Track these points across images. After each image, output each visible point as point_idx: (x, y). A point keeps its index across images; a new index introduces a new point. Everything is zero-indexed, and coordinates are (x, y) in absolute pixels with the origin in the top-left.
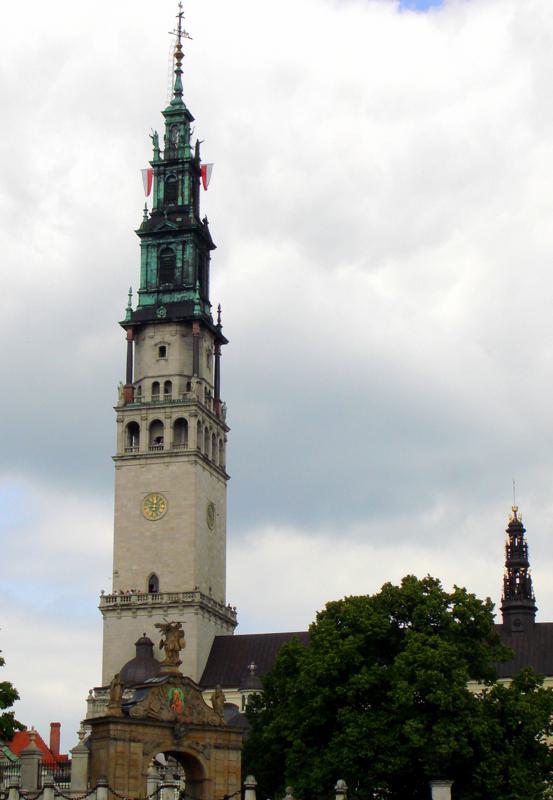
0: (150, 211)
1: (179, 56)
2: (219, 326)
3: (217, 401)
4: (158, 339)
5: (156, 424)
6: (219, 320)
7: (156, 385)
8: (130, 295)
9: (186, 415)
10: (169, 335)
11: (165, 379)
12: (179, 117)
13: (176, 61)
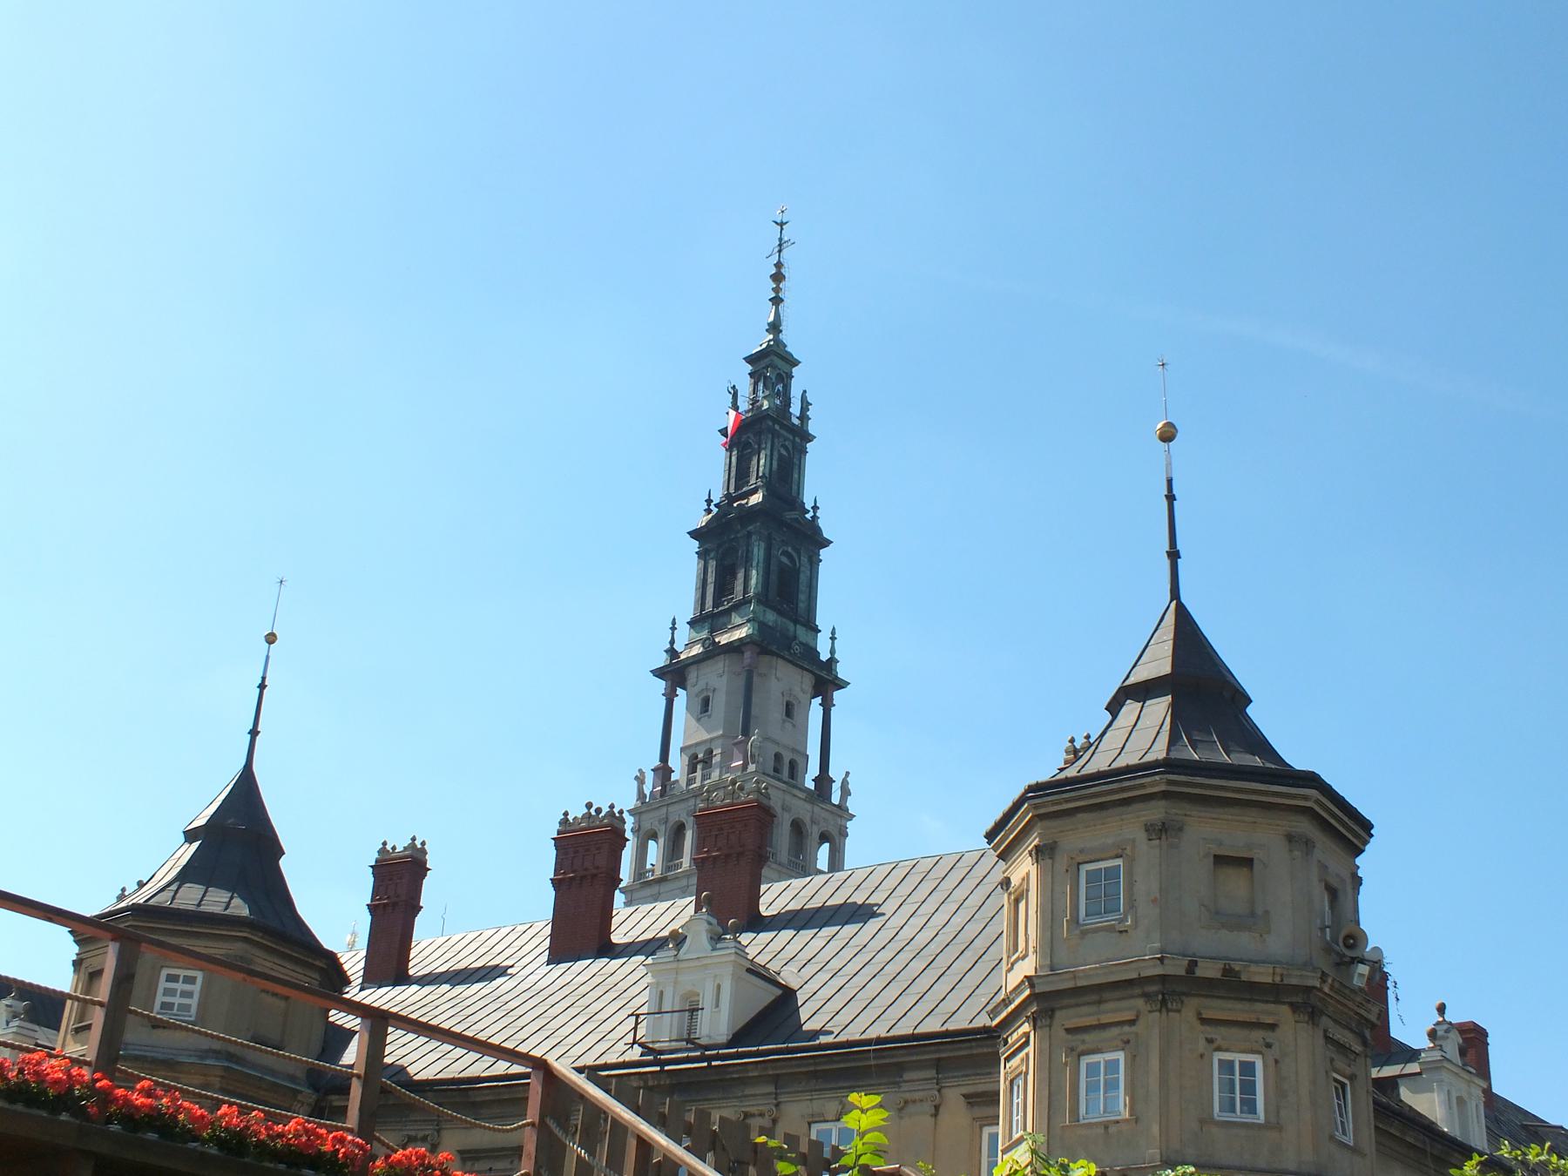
1: (778, 277)
2: (832, 661)
3: (824, 780)
4: (701, 685)
6: (832, 651)
8: (673, 629)
11: (704, 748)
12: (772, 365)
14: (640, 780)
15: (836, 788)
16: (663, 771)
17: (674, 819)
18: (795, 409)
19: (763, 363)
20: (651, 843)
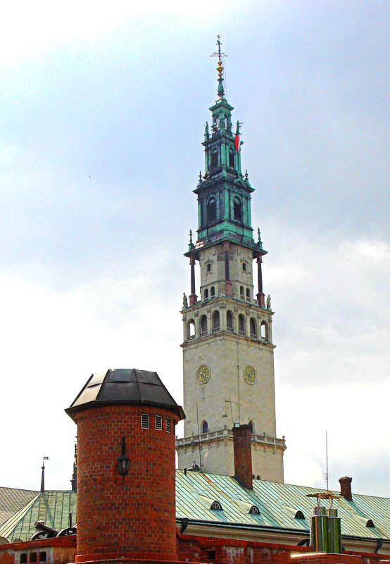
0: (204, 175)
1: (220, 70)
2: (260, 243)
3: (260, 295)
5: (204, 318)
6: (259, 239)
7: (206, 291)
8: (191, 235)
9: (218, 309)
10: (211, 255)
11: (211, 286)
12: (222, 110)
13: (222, 77)
14: (185, 299)
15: (266, 298)
16: (194, 296)
17: (201, 314)
18: (234, 130)
19: (218, 110)
20: (192, 325)
